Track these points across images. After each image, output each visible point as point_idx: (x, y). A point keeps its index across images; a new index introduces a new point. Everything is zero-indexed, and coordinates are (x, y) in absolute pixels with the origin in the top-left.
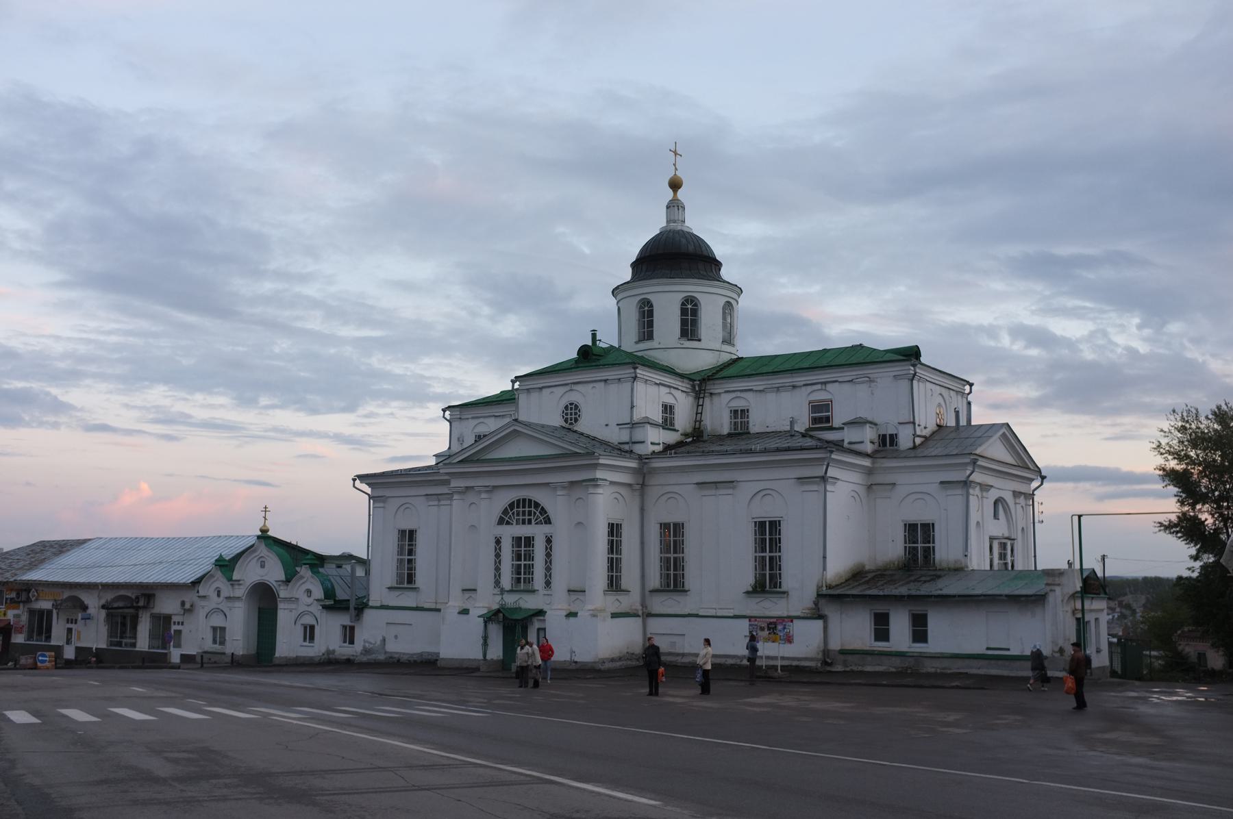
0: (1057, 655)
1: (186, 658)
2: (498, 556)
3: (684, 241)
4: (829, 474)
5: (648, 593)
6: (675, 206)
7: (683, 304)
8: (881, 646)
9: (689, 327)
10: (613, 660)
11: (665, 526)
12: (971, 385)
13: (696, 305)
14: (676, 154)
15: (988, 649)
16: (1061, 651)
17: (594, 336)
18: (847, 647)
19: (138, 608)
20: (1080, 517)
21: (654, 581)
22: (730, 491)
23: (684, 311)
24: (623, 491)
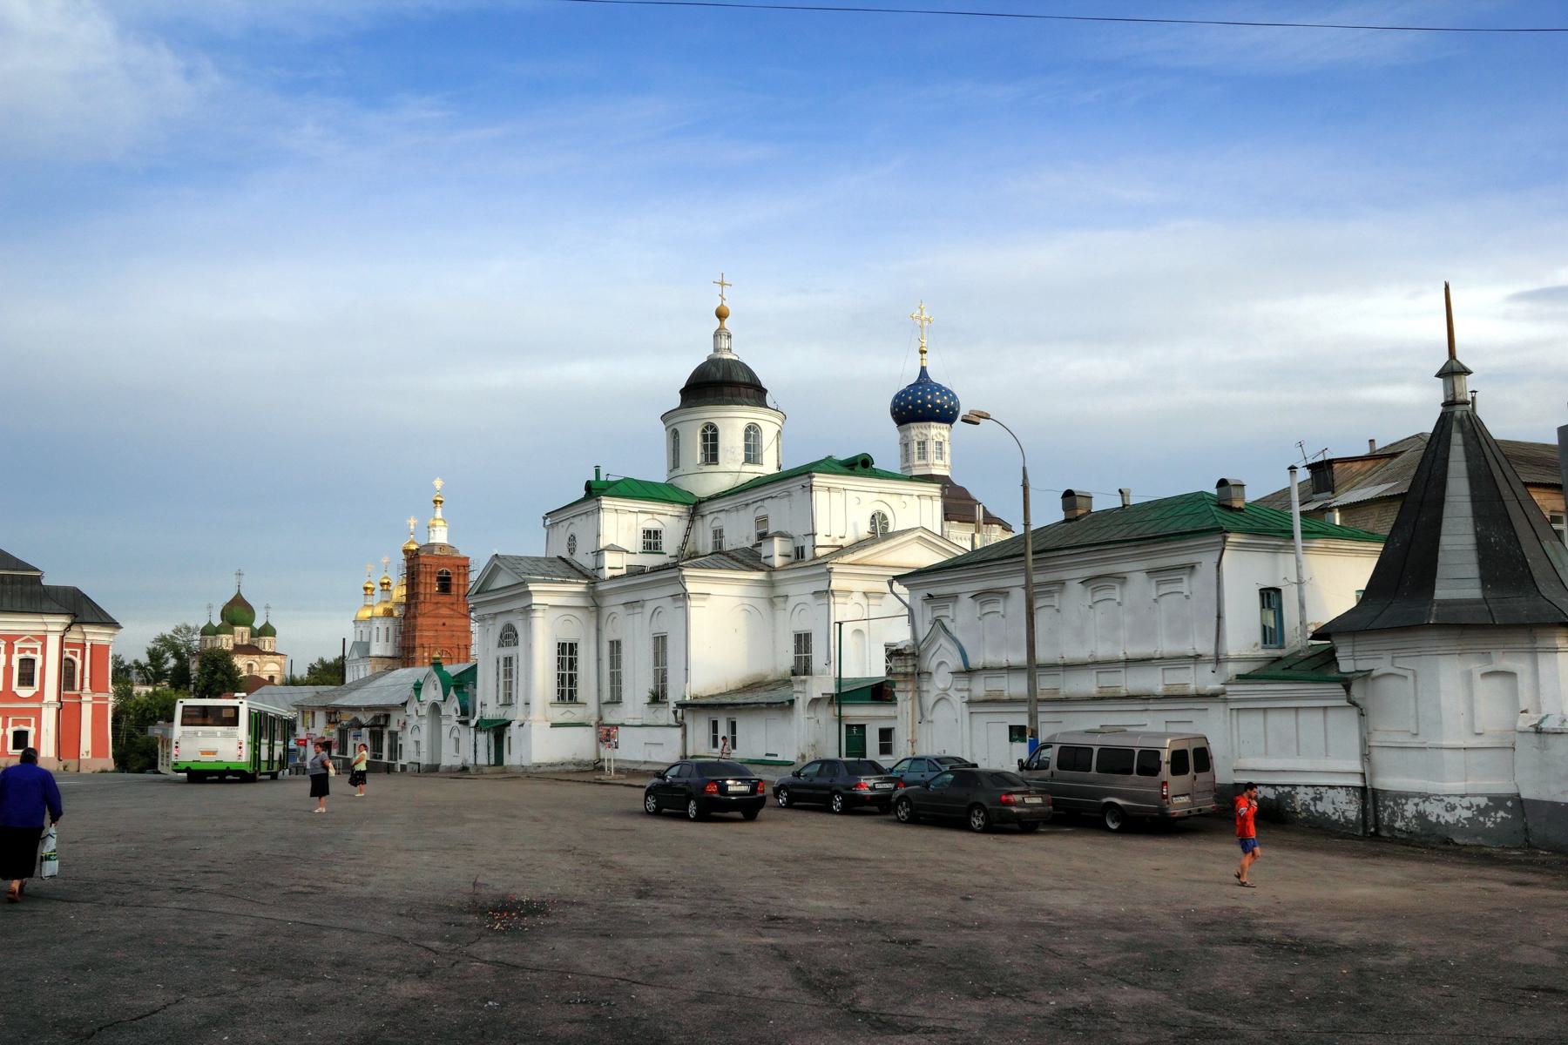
1: (403, 768)
4: (833, 586)
5: (602, 704)
9: (711, 453)
10: (551, 765)
11: (612, 642)
16: (803, 757)
17: (597, 472)
19: (382, 726)
21: (606, 696)
23: (705, 438)
24: (577, 613)
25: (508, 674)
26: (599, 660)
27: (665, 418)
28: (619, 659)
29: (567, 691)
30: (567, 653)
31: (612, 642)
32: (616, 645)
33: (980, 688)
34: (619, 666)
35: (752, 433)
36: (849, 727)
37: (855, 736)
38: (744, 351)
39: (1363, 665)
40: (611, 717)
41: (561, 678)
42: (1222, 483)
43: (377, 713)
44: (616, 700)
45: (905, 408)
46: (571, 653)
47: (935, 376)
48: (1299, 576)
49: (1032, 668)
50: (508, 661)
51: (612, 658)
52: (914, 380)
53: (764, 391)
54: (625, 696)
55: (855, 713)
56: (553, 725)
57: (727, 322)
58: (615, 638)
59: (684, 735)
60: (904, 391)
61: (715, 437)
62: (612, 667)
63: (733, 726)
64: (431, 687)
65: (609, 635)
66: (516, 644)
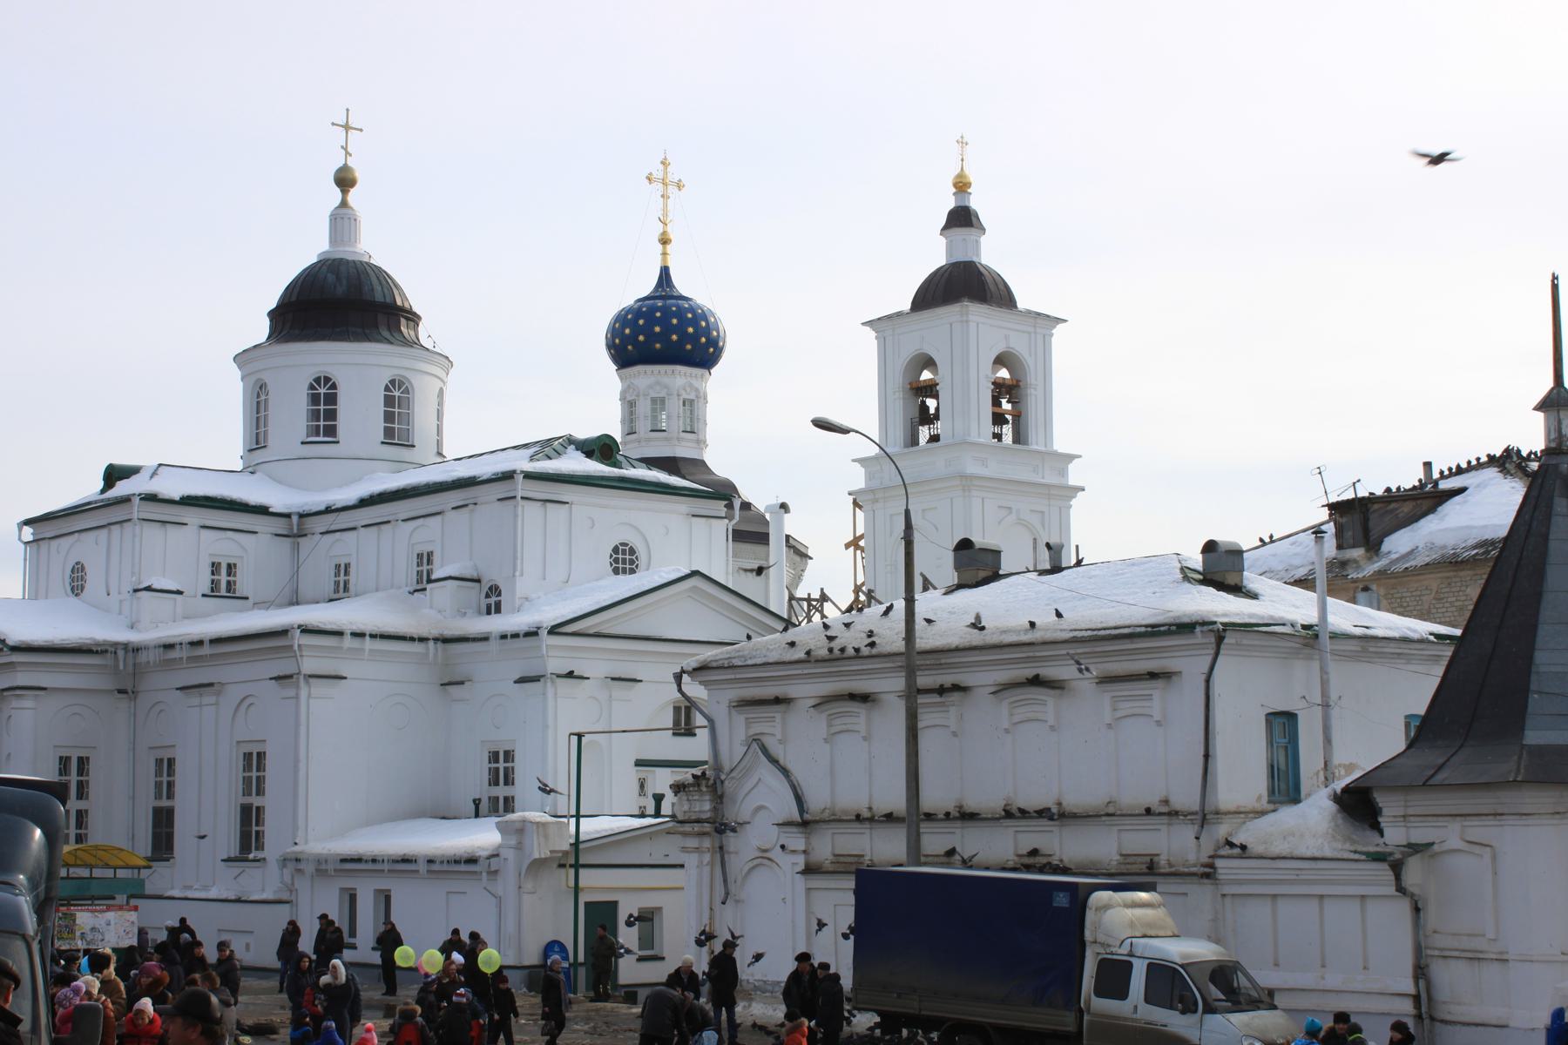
3: (331, 278)
6: (342, 220)
7: (312, 387)
13: (334, 386)
14: (347, 127)
20: (580, 736)
22: (212, 699)
23: (315, 399)
27: (242, 359)
33: (825, 846)
38: (378, 246)
39: (1419, 835)
42: (1210, 547)
45: (633, 339)
46: (81, 771)
47: (683, 285)
48: (1325, 694)
49: (915, 818)
52: (646, 285)
53: (413, 318)
57: (354, 196)
60: (628, 310)
61: (332, 399)
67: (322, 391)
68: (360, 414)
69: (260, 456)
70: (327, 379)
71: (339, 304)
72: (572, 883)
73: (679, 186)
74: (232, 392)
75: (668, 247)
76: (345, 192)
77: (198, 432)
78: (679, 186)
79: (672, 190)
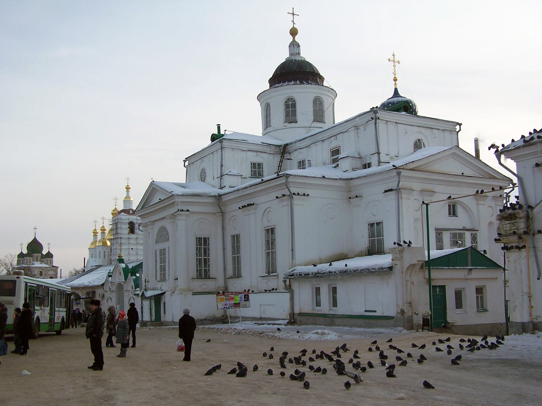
0: (399, 315)
2: (156, 261)
5: (226, 279)
6: (294, 45)
7: (286, 102)
8: (318, 310)
11: (233, 237)
12: (460, 125)
13: (294, 101)
14: (293, 14)
15: (366, 311)
16: (402, 312)
18: (303, 312)
20: (427, 205)
21: (230, 272)
23: (287, 106)
25: (163, 261)
26: (224, 249)
28: (238, 247)
29: (203, 272)
30: (203, 244)
31: (233, 237)
32: (236, 239)
34: (238, 252)
35: (318, 103)
36: (435, 287)
37: (438, 295)
38: (307, 54)
40: (236, 286)
41: (199, 261)
43: (88, 290)
44: (237, 275)
50: (163, 252)
51: (233, 247)
53: (322, 79)
54: (244, 272)
55: (439, 275)
56: (195, 294)
57: (297, 38)
58: (235, 233)
59: (292, 299)
61: (294, 106)
62: (234, 253)
63: (334, 290)
64: (118, 274)
65: (230, 232)
66: (168, 240)
67: (290, 103)
68: (305, 110)
69: (269, 129)
70: (292, 99)
71: (295, 72)
72: (427, 277)
73: (399, 62)
74: (257, 110)
75: (397, 82)
76: (294, 40)
77: (246, 121)
78: (399, 62)
79: (396, 64)
